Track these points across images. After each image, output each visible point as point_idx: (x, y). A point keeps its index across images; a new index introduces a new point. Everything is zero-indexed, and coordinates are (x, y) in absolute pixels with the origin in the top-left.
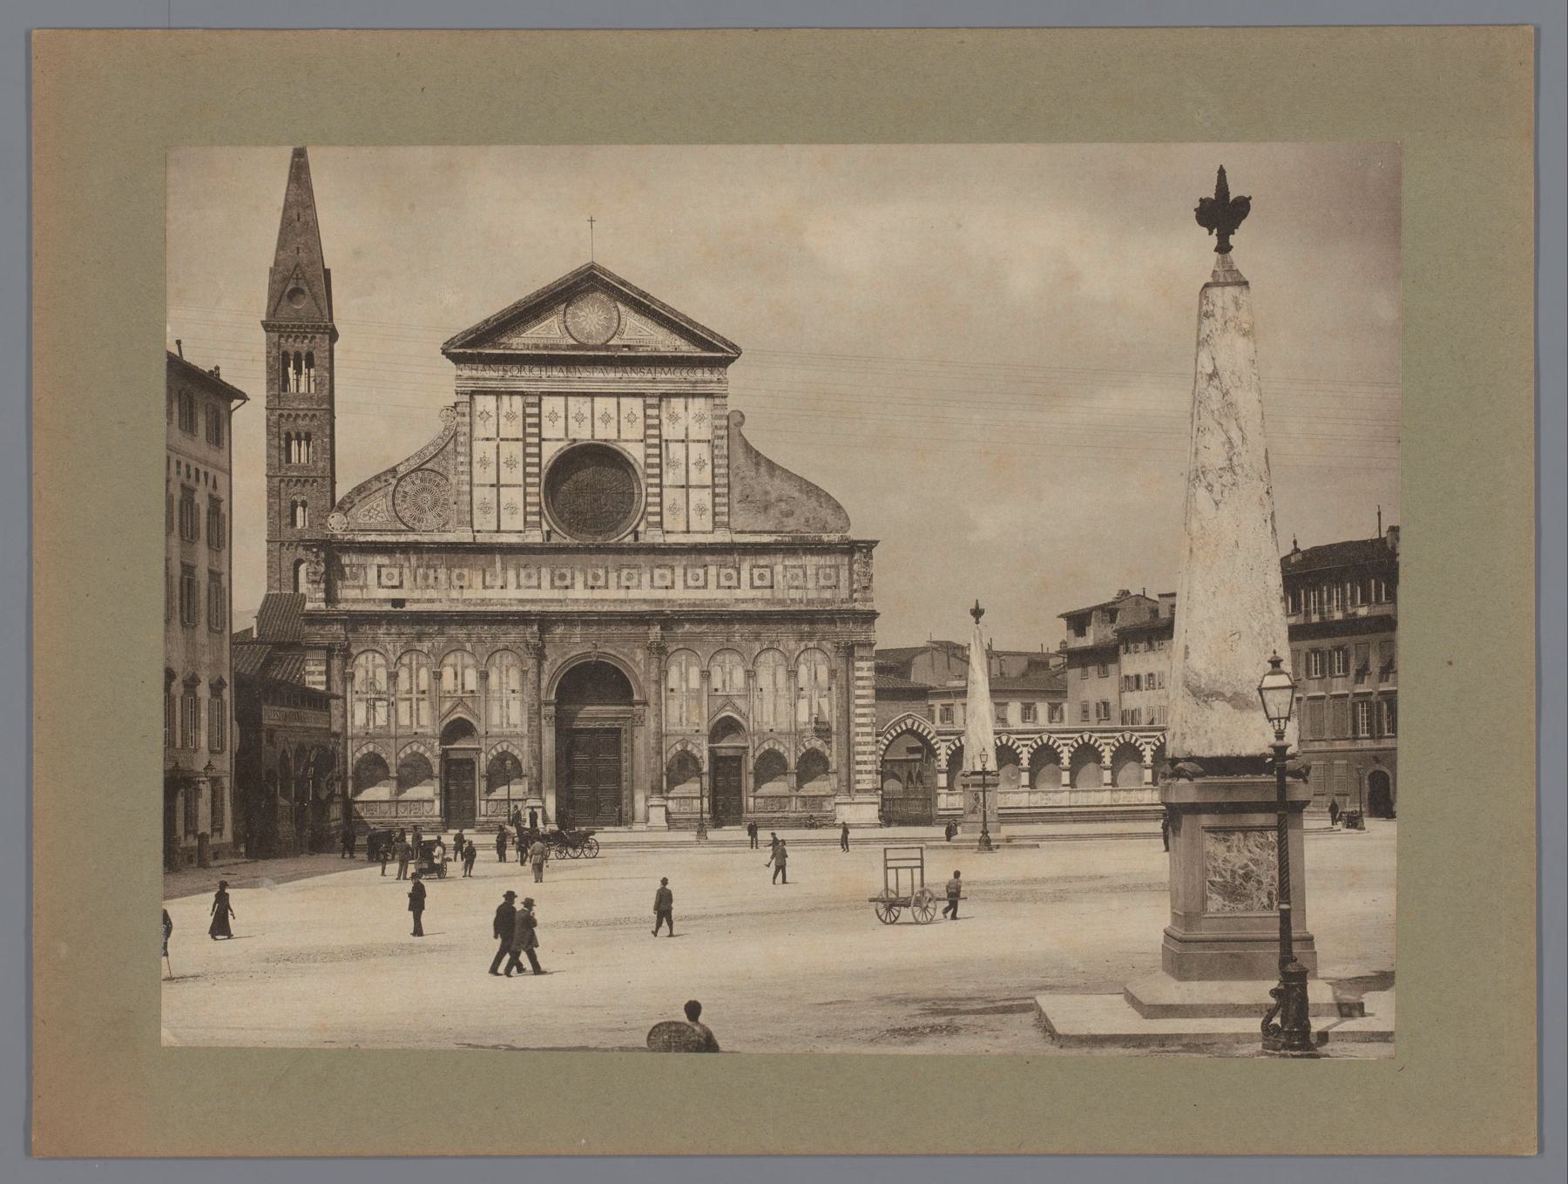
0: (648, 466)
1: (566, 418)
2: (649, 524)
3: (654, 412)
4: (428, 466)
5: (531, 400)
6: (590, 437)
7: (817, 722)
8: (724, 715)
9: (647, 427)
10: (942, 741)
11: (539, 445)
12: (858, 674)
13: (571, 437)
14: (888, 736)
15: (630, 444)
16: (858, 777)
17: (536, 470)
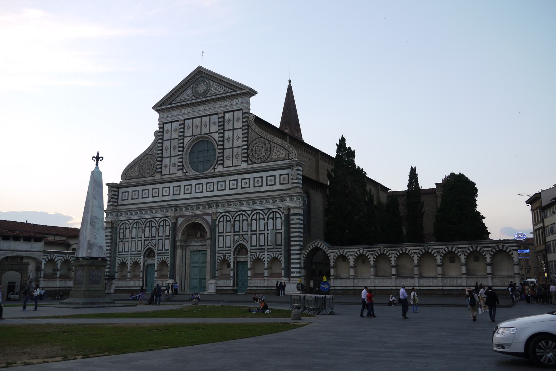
0: (219, 141)
1: (193, 127)
2: (219, 164)
3: (222, 120)
4: (150, 153)
5: (181, 123)
6: (200, 134)
7: (276, 245)
8: (239, 243)
9: (219, 126)
10: (331, 252)
11: (183, 139)
12: (292, 222)
13: (193, 135)
14: (307, 250)
15: (213, 134)
16: (292, 270)
17: (181, 149)
